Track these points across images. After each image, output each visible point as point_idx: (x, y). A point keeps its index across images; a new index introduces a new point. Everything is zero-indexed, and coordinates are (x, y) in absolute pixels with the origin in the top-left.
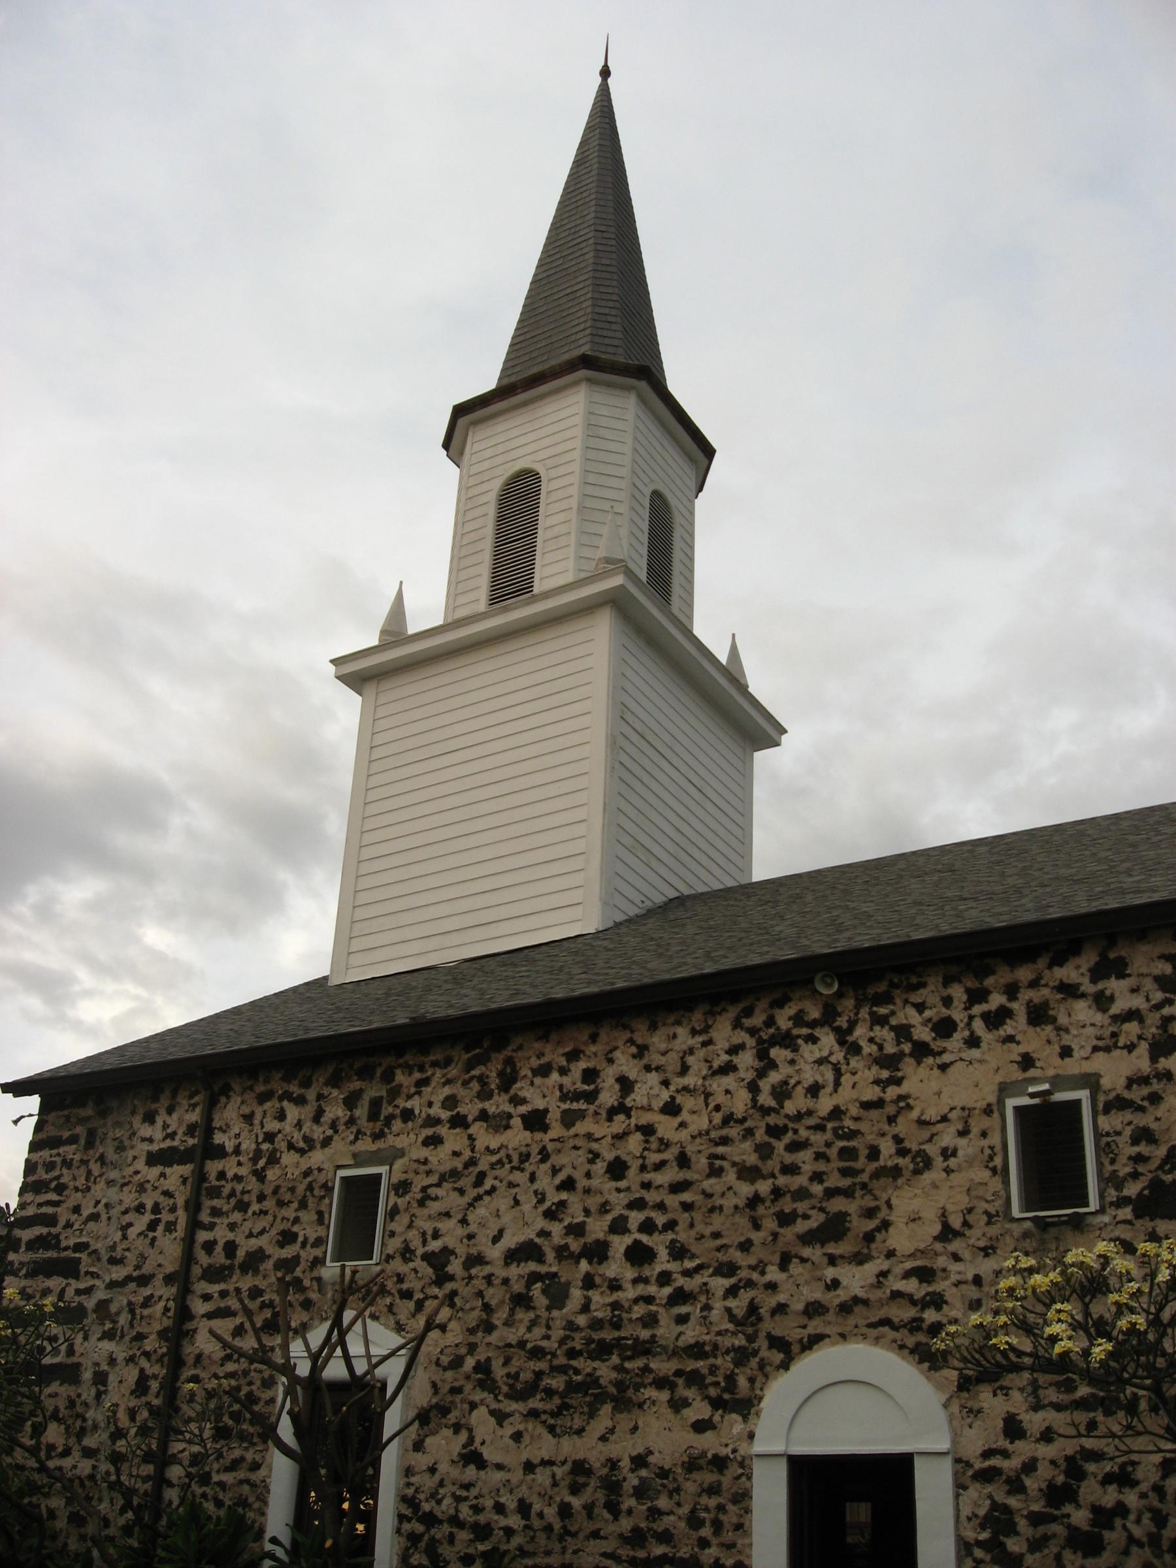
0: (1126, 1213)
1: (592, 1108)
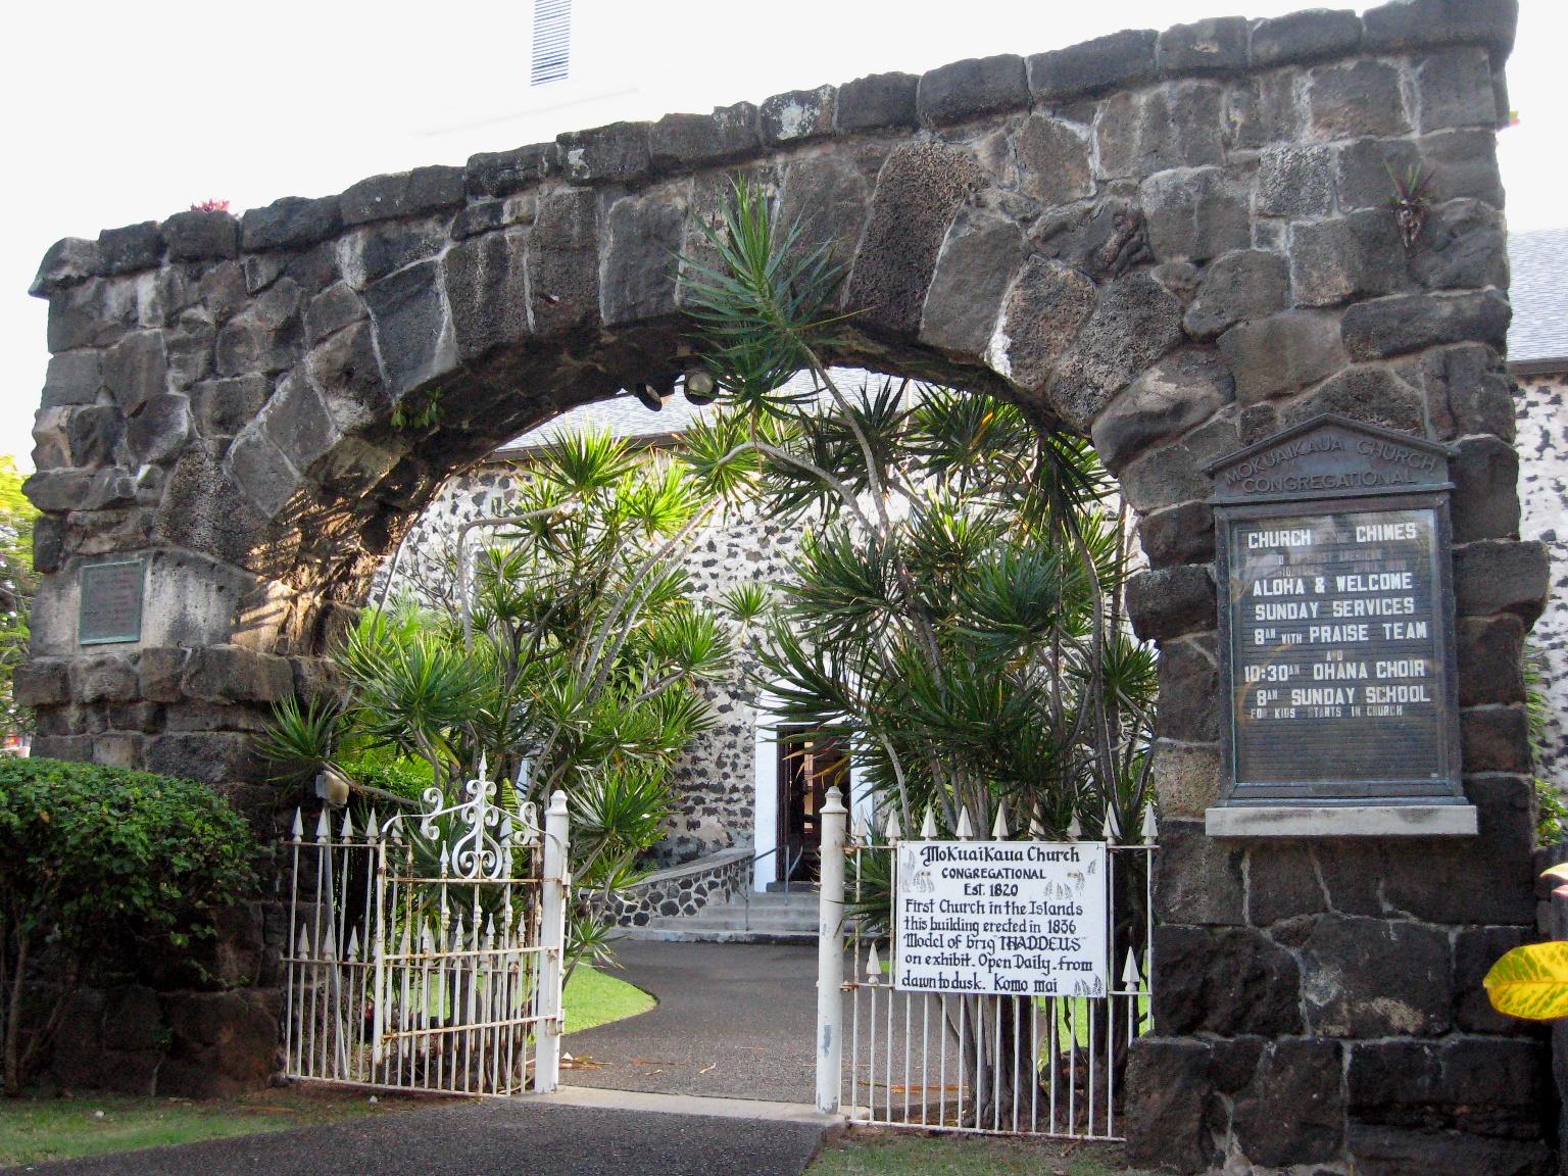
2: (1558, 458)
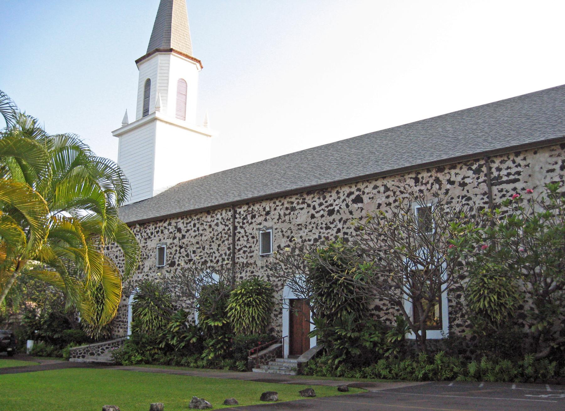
2: (282, 222)
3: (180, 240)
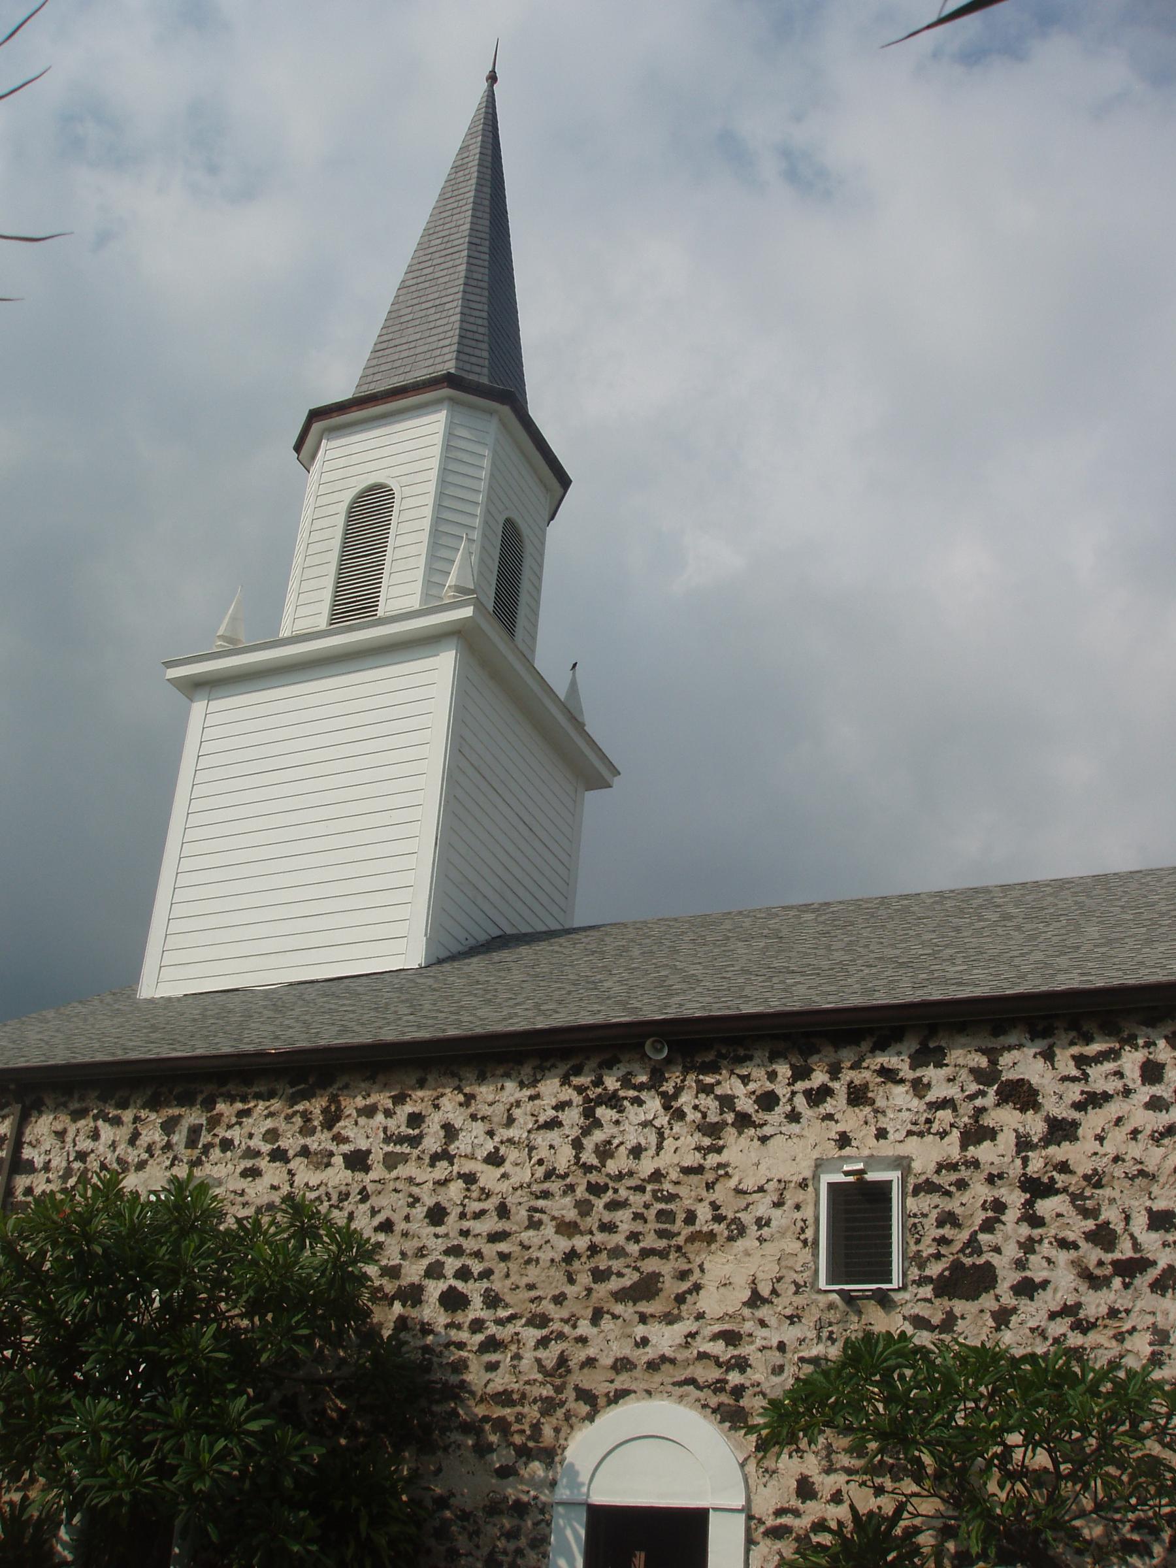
0: (927, 1291)
1: (416, 1152)
3: (1023, 1144)
